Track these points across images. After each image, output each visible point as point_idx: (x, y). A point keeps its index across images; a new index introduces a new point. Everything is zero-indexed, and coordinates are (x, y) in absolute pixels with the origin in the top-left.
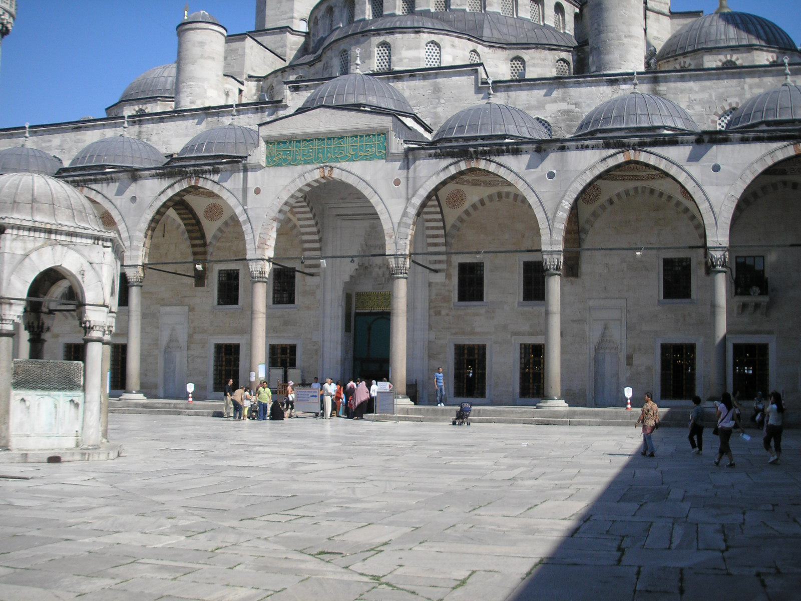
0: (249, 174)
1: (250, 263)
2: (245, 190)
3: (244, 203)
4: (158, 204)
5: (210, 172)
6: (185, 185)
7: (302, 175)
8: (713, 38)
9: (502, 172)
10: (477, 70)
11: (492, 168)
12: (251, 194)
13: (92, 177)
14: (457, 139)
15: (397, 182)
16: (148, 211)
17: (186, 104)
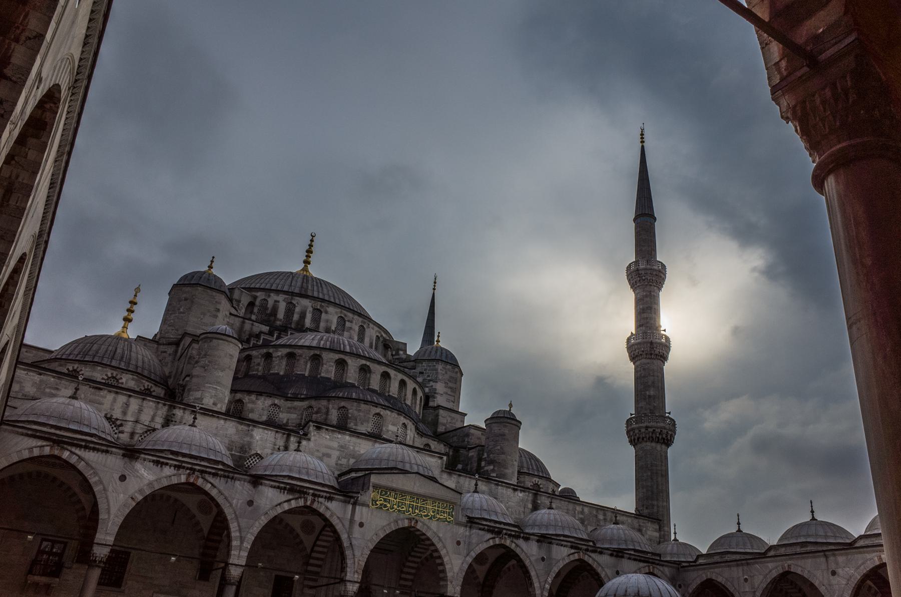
0: (357, 507)
1: (348, 584)
2: (352, 521)
3: (350, 533)
4: (273, 514)
5: (326, 498)
6: (301, 503)
7: (396, 521)
8: (525, 465)
9: (518, 551)
10: (441, 458)
11: (513, 546)
12: (356, 527)
13: (213, 471)
14: (490, 521)
15: (458, 543)
16: (263, 518)
17: (208, 402)
